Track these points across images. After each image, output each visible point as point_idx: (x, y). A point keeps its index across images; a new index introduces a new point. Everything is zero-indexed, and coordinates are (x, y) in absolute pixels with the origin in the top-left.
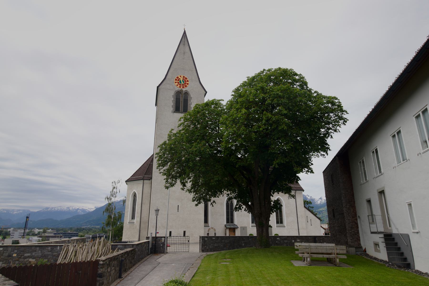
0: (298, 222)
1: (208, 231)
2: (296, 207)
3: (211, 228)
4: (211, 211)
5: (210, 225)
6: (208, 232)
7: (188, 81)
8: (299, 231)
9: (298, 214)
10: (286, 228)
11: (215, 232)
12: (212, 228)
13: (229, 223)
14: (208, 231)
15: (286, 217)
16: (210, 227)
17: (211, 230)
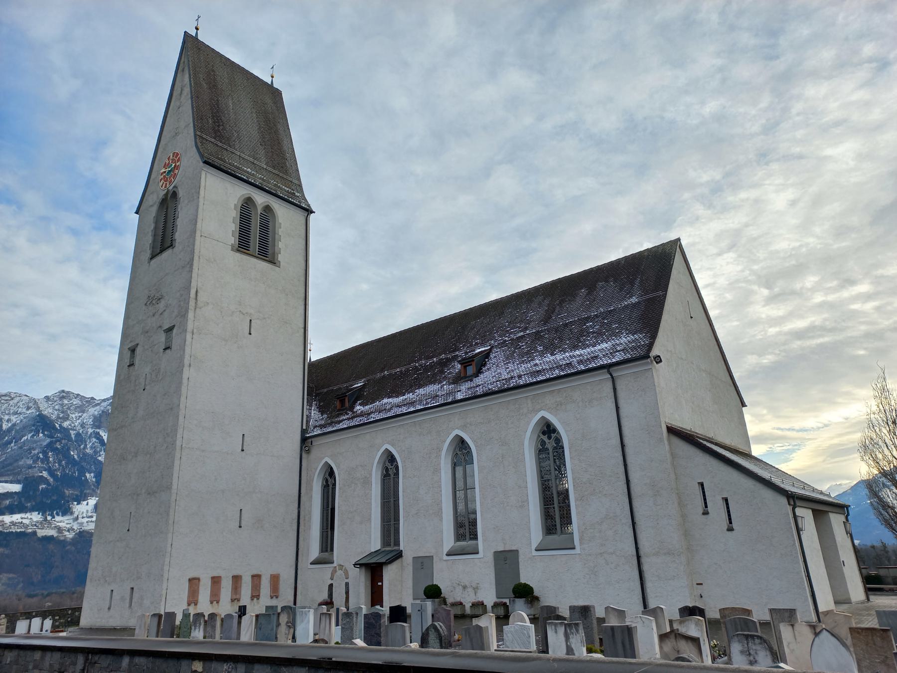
0: (637, 520)
1: (330, 576)
2: (623, 446)
3: (337, 567)
4: (339, 507)
5: (335, 559)
6: (330, 582)
7: (178, 160)
8: (645, 568)
9: (631, 478)
10: (578, 550)
11: (347, 581)
12: (341, 566)
13: (390, 545)
14: (332, 579)
15: (576, 500)
16: (335, 564)
17: (337, 573)
